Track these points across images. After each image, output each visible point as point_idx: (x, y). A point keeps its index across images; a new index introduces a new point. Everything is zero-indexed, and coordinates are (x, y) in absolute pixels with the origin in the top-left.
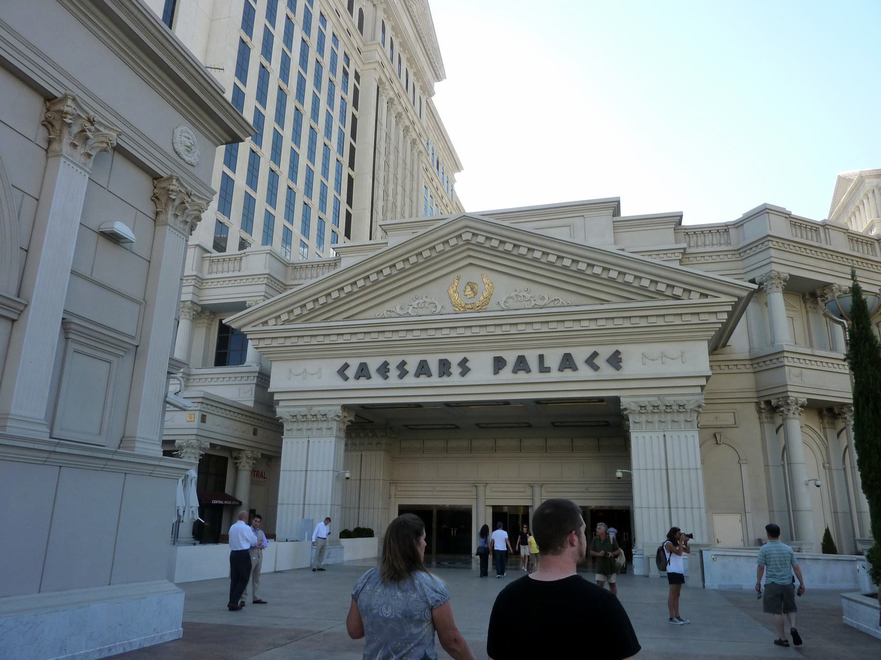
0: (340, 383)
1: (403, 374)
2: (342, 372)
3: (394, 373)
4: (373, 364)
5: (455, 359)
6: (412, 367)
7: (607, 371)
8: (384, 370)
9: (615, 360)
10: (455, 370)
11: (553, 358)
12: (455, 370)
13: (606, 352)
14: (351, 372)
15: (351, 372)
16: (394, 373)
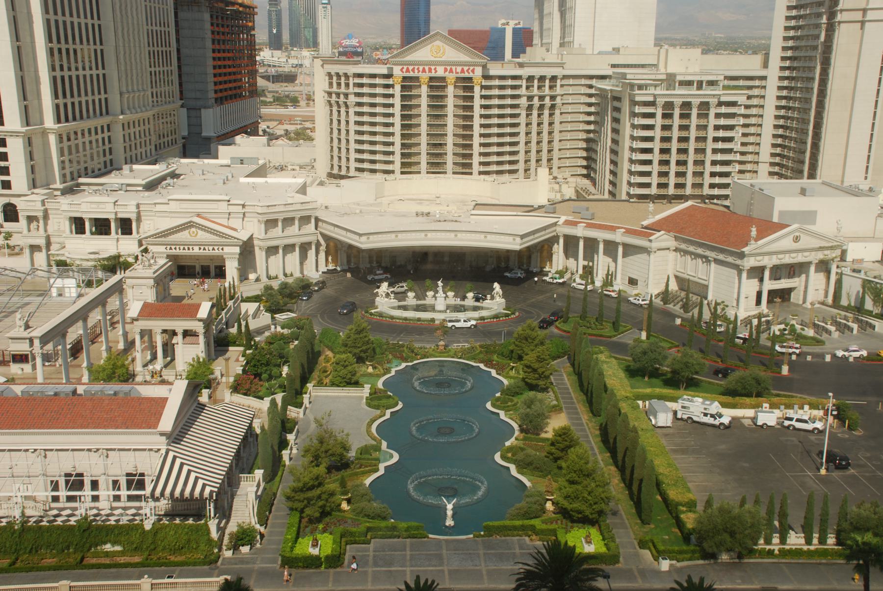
0: (401, 73)
1: (419, 72)
2: (402, 70)
3: (416, 71)
4: (411, 68)
5: (433, 68)
6: (421, 69)
8: (413, 70)
9: (473, 71)
10: (433, 71)
11: (459, 69)
12: (433, 71)
13: (471, 68)
14: (404, 70)
15: (404, 70)
16: (416, 71)
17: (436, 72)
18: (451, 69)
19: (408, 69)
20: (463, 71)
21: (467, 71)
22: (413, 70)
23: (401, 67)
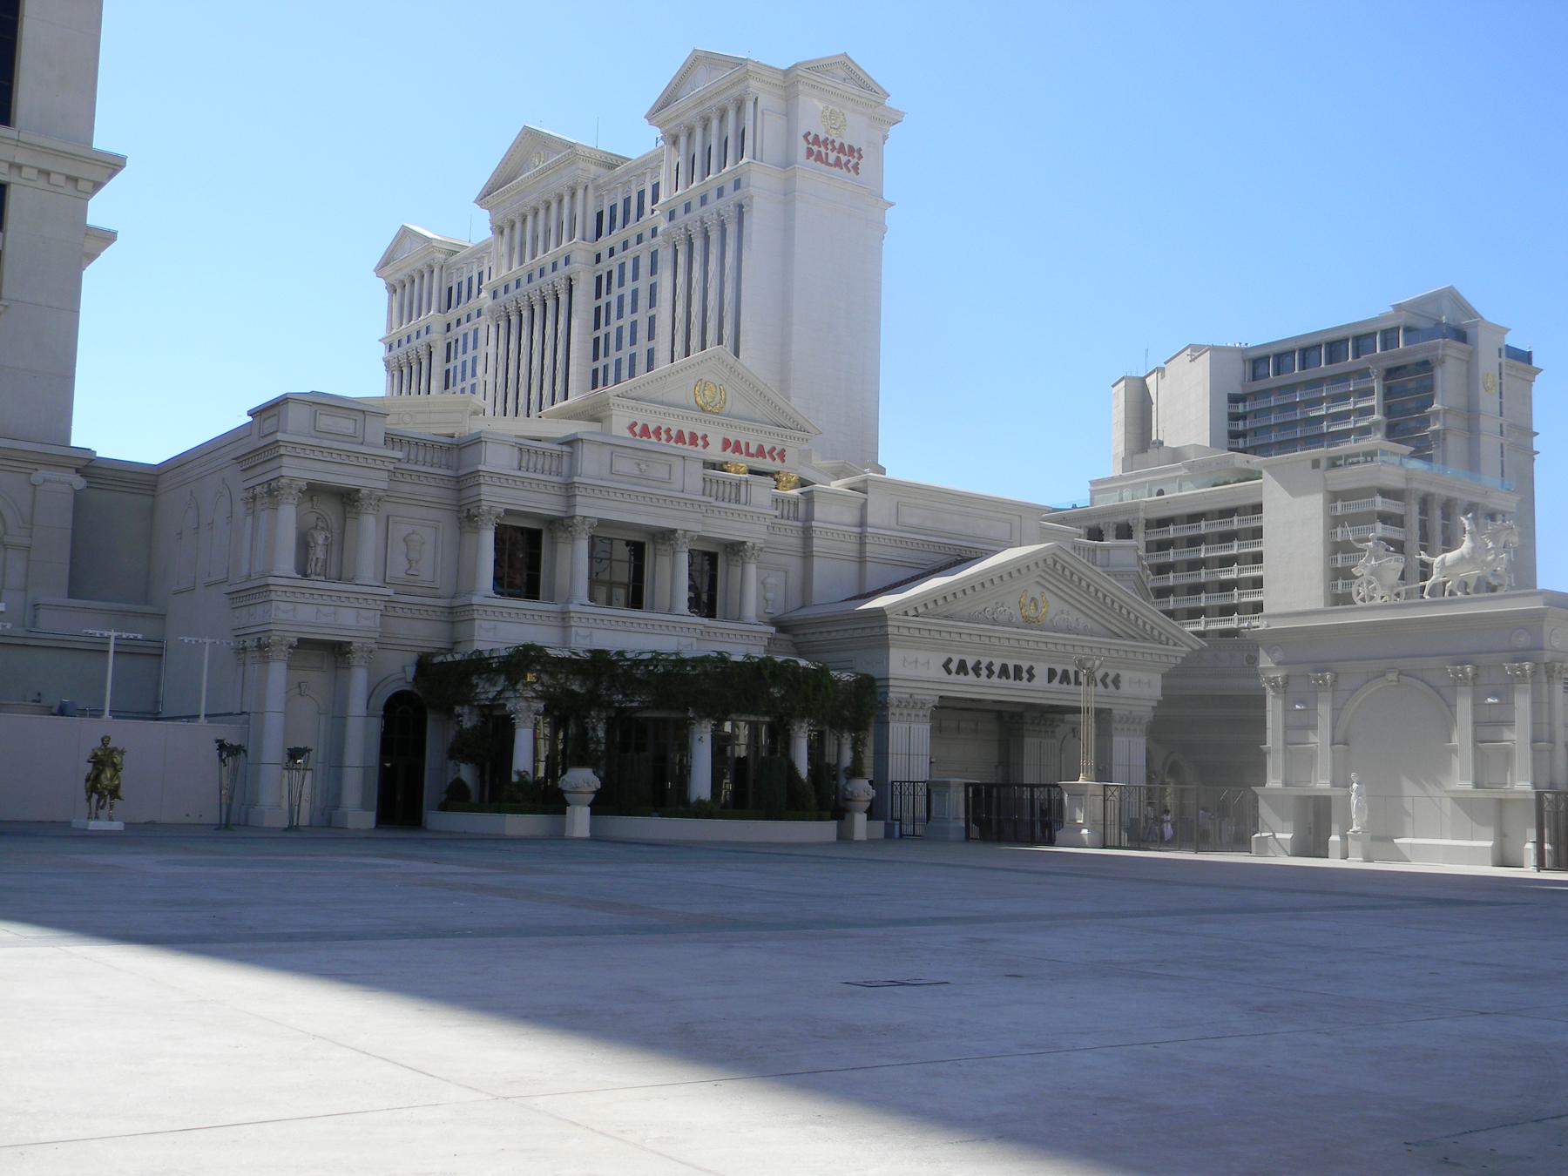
0: (628, 434)
1: (669, 439)
2: (632, 427)
5: (700, 435)
7: (778, 461)
9: (782, 455)
10: (700, 442)
11: (753, 450)
13: (778, 449)
14: (637, 429)
16: (664, 436)
17: (706, 445)
18: (738, 443)
19: (645, 427)
20: (761, 452)
21: (771, 453)
22: (658, 431)
23: (628, 422)
